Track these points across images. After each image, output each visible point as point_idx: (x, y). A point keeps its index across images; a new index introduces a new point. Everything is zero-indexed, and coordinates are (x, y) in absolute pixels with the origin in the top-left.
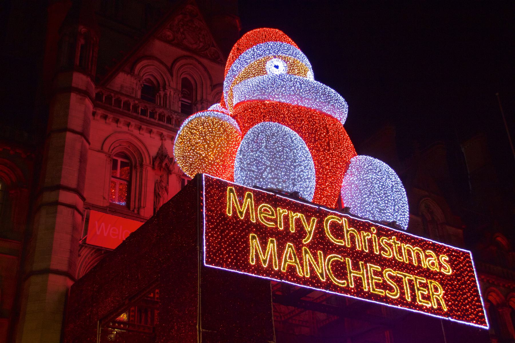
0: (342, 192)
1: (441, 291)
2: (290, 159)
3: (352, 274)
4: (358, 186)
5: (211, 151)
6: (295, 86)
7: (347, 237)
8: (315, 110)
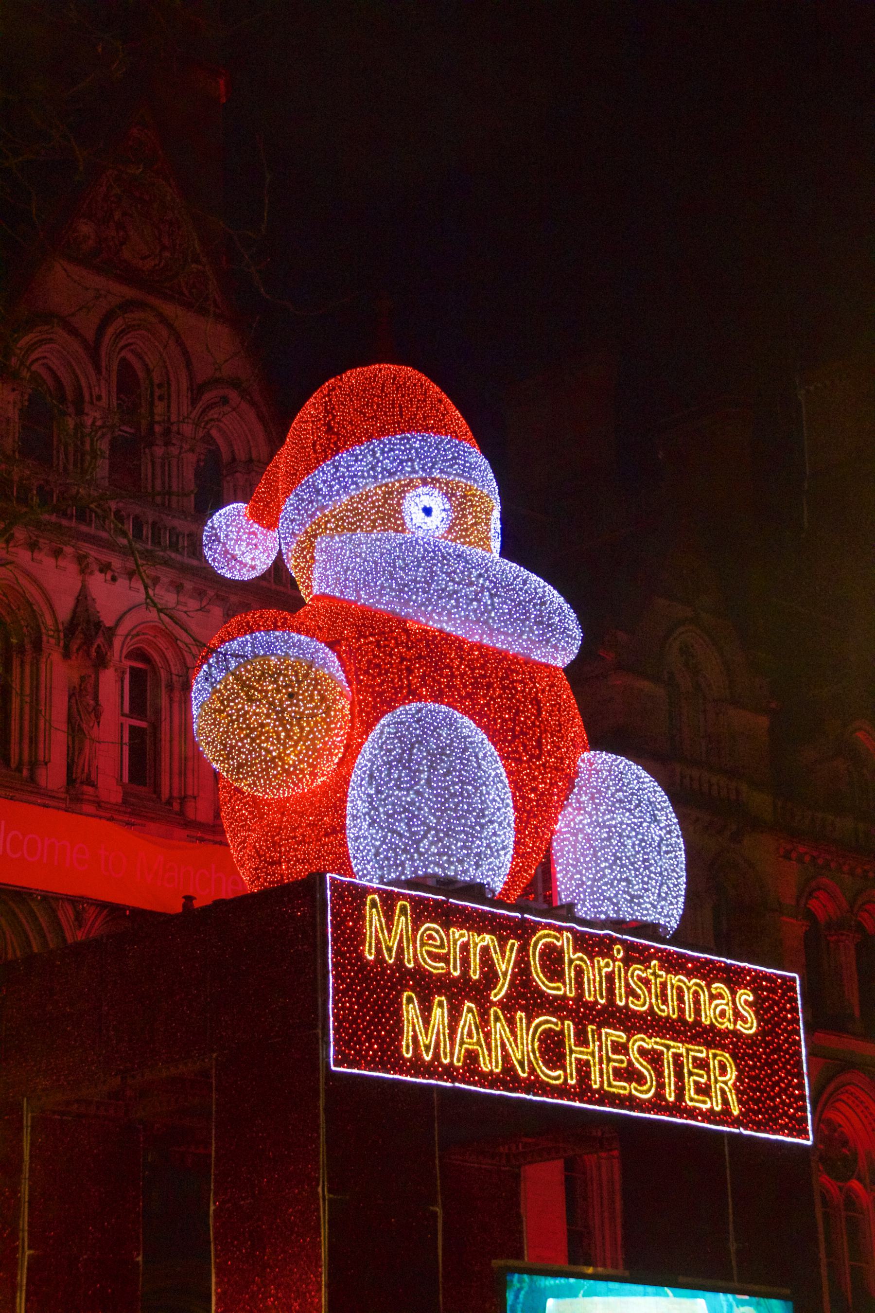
0: (555, 844)
1: (732, 1074)
2: (474, 810)
3: (574, 1055)
4: (591, 839)
5: (291, 746)
6: (479, 601)
7: (570, 974)
8: (515, 656)
